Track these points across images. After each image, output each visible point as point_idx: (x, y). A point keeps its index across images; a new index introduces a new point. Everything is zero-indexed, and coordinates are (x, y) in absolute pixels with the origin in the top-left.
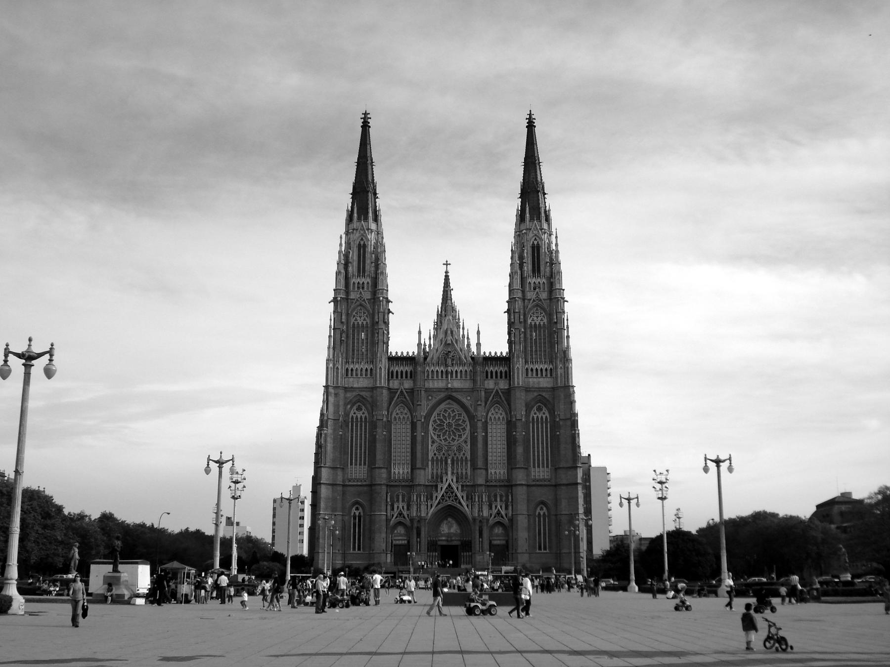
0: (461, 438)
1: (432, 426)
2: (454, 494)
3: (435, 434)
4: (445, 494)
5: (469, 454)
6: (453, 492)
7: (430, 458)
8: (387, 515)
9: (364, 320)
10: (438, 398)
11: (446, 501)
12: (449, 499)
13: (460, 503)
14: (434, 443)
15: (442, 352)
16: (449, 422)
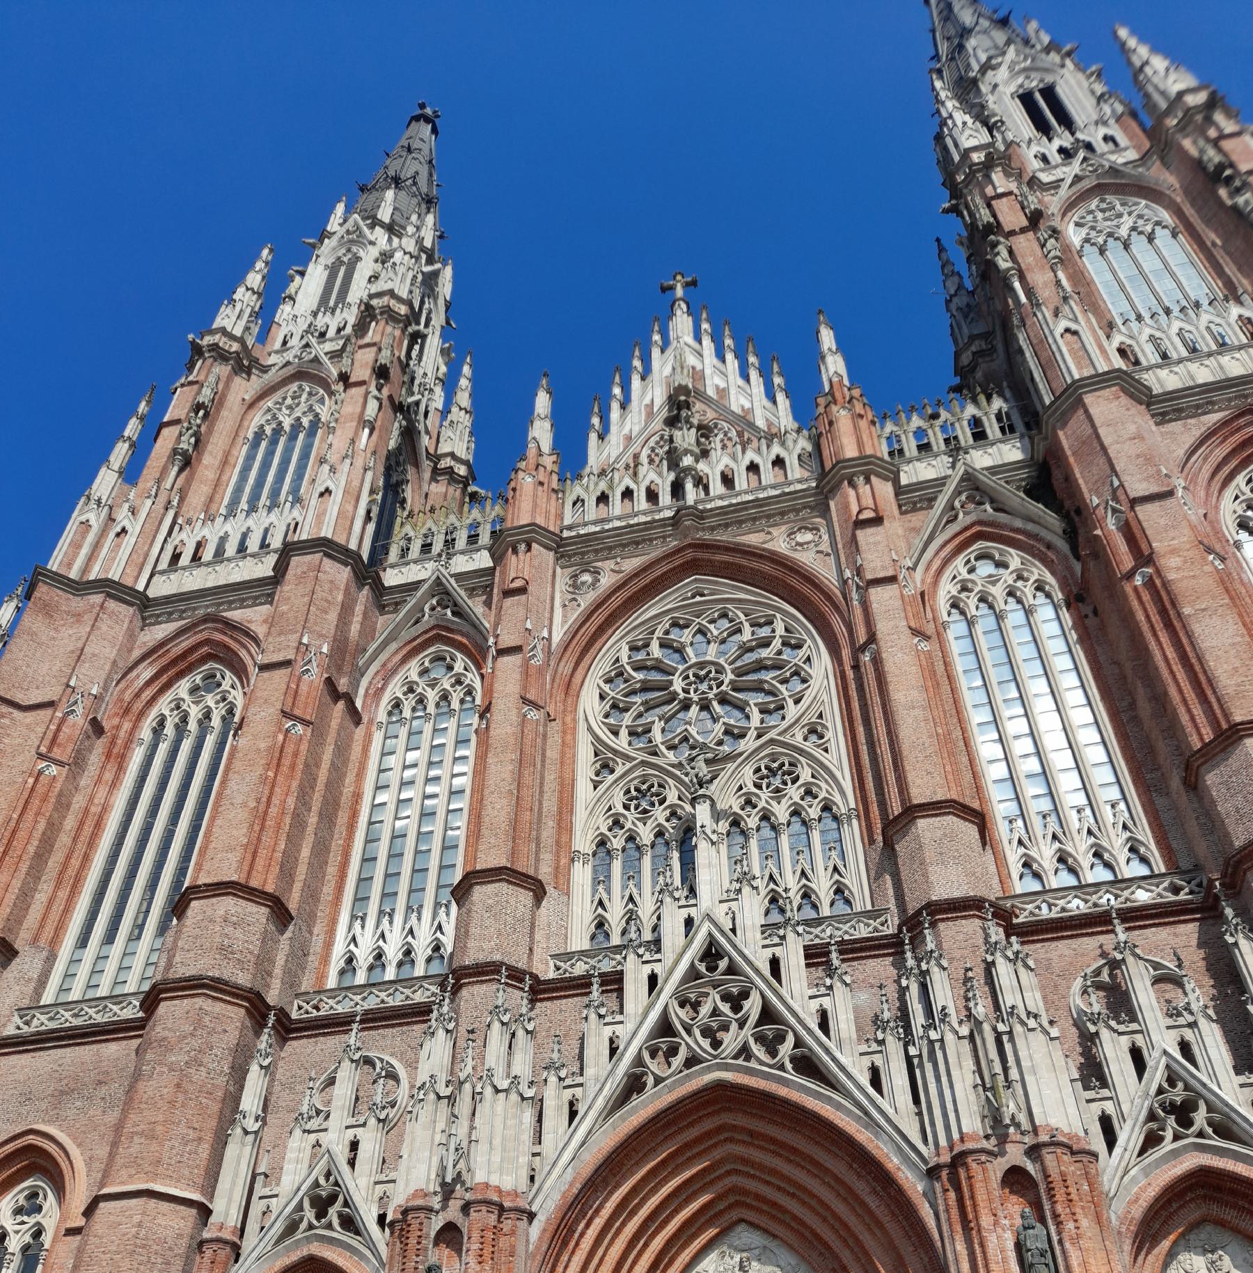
0: (783, 718)
1: (602, 697)
2: (752, 1006)
3: (616, 733)
4: (680, 1015)
5: (848, 785)
6: (745, 995)
7: (583, 842)
8: (205, 1212)
9: (311, 409)
10: (631, 564)
11: (691, 1061)
12: (716, 1044)
13: (807, 1065)
14: (612, 771)
15: (656, 438)
16: (701, 665)
